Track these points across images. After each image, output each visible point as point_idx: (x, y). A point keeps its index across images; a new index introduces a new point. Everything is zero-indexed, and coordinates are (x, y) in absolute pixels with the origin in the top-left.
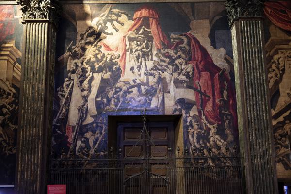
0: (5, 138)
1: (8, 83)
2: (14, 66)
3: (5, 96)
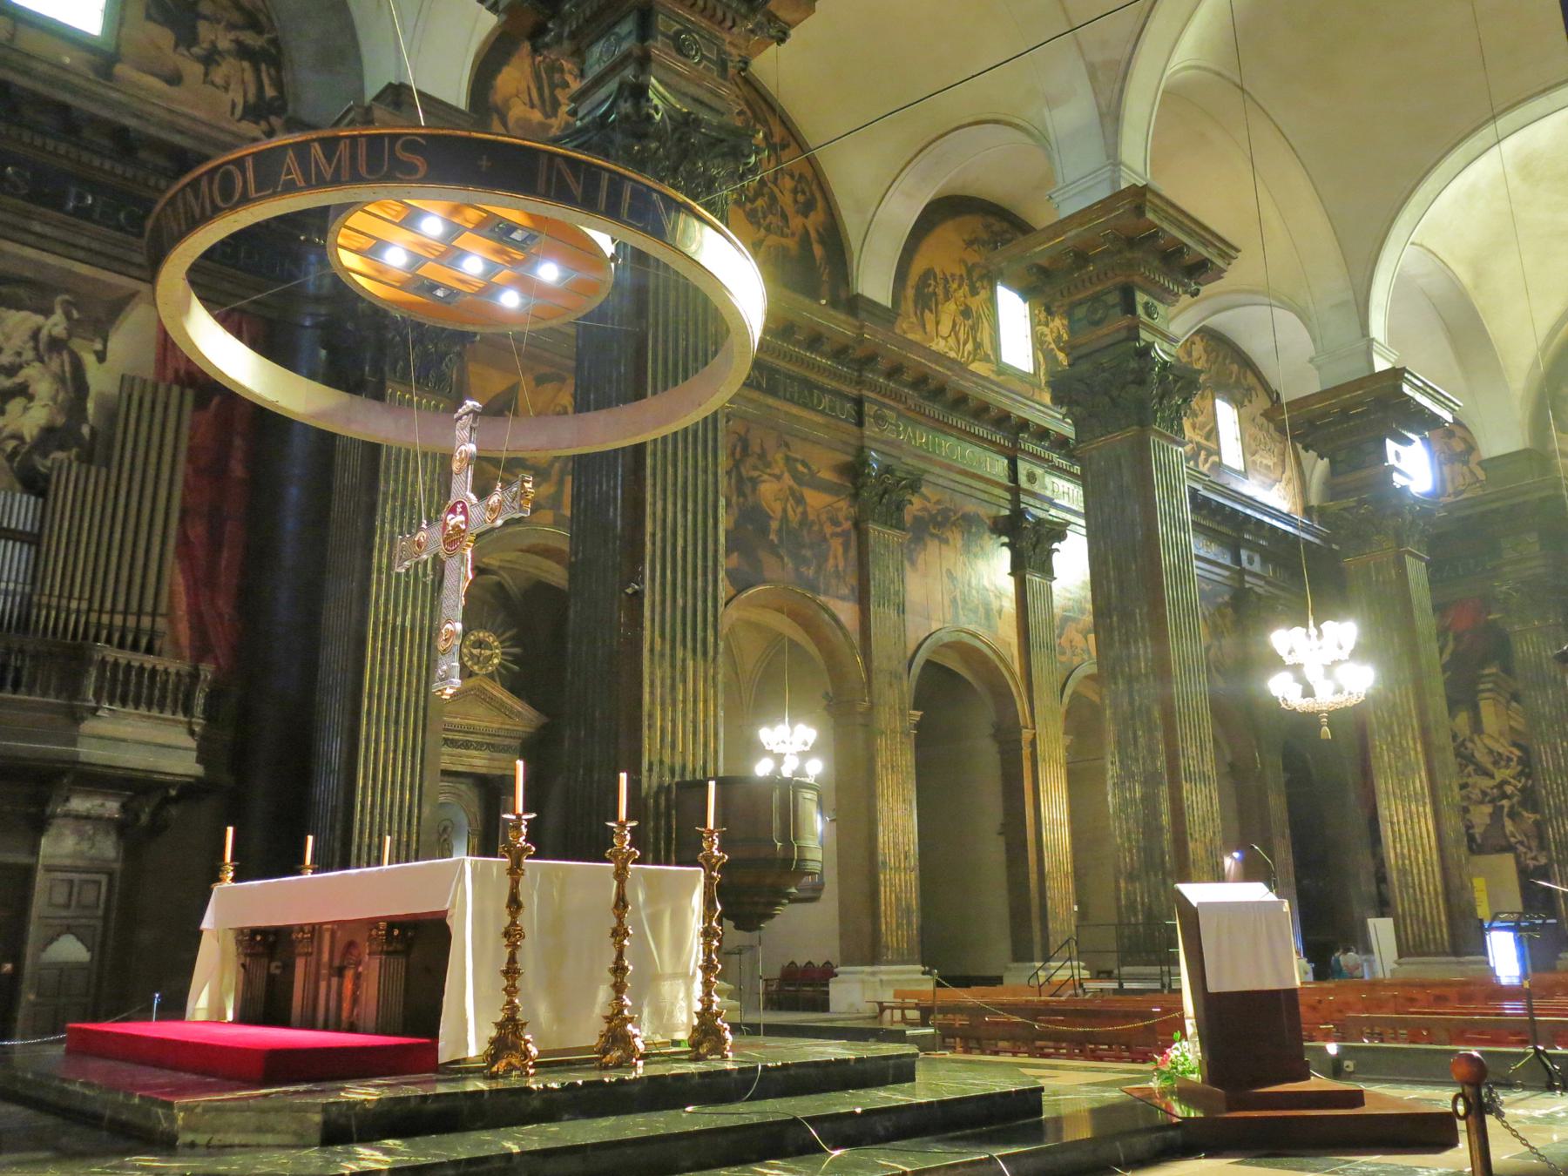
0: (1519, 838)
1: (1502, 740)
2: (1508, 708)
3: (1503, 763)
